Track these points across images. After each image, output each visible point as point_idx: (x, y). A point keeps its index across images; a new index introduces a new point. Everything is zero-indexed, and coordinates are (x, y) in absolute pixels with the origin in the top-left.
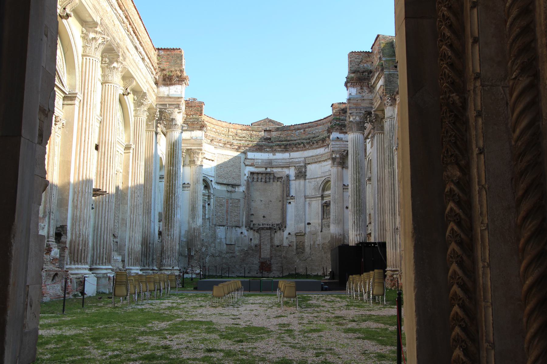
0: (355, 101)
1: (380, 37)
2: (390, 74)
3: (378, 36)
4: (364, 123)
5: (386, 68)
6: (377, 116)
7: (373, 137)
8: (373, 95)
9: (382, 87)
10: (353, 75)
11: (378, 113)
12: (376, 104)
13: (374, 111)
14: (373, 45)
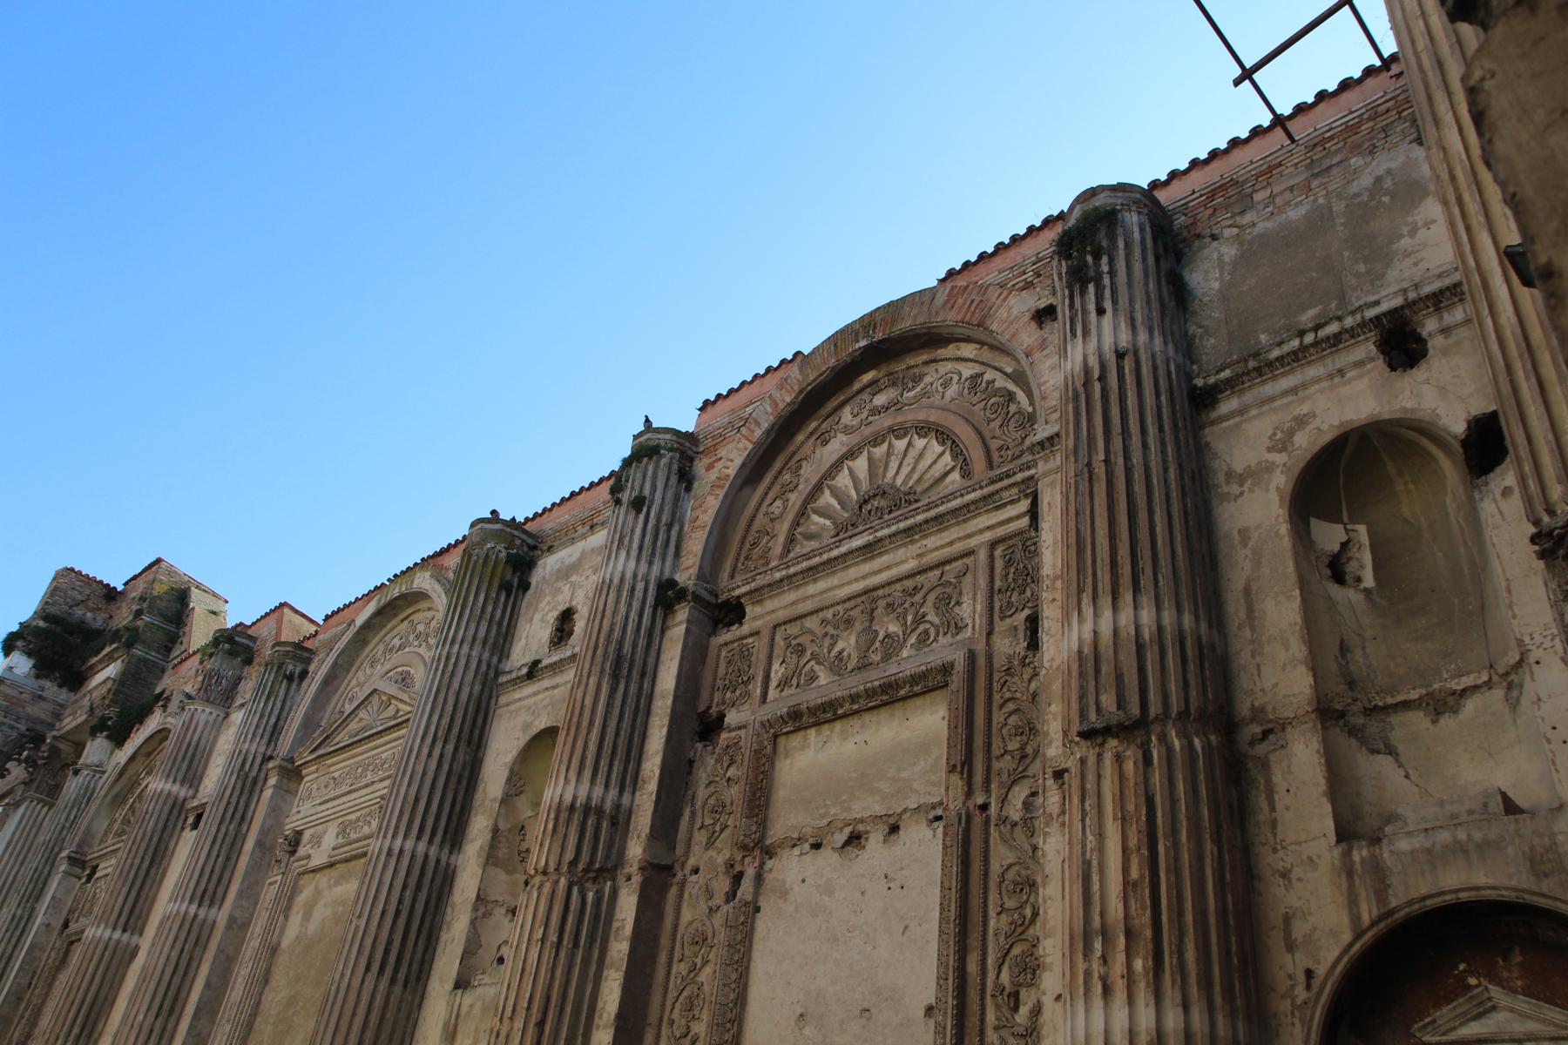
0: (13, 693)
1: (163, 565)
2: (146, 661)
3: (159, 561)
4: (10, 759)
5: (143, 642)
6: (55, 751)
7: (17, 805)
8: (72, 697)
9: (109, 684)
10: (42, 624)
11: (61, 746)
12: (69, 723)
13: (55, 738)
14: (135, 578)
